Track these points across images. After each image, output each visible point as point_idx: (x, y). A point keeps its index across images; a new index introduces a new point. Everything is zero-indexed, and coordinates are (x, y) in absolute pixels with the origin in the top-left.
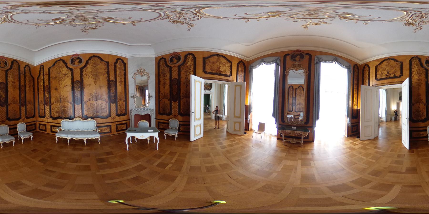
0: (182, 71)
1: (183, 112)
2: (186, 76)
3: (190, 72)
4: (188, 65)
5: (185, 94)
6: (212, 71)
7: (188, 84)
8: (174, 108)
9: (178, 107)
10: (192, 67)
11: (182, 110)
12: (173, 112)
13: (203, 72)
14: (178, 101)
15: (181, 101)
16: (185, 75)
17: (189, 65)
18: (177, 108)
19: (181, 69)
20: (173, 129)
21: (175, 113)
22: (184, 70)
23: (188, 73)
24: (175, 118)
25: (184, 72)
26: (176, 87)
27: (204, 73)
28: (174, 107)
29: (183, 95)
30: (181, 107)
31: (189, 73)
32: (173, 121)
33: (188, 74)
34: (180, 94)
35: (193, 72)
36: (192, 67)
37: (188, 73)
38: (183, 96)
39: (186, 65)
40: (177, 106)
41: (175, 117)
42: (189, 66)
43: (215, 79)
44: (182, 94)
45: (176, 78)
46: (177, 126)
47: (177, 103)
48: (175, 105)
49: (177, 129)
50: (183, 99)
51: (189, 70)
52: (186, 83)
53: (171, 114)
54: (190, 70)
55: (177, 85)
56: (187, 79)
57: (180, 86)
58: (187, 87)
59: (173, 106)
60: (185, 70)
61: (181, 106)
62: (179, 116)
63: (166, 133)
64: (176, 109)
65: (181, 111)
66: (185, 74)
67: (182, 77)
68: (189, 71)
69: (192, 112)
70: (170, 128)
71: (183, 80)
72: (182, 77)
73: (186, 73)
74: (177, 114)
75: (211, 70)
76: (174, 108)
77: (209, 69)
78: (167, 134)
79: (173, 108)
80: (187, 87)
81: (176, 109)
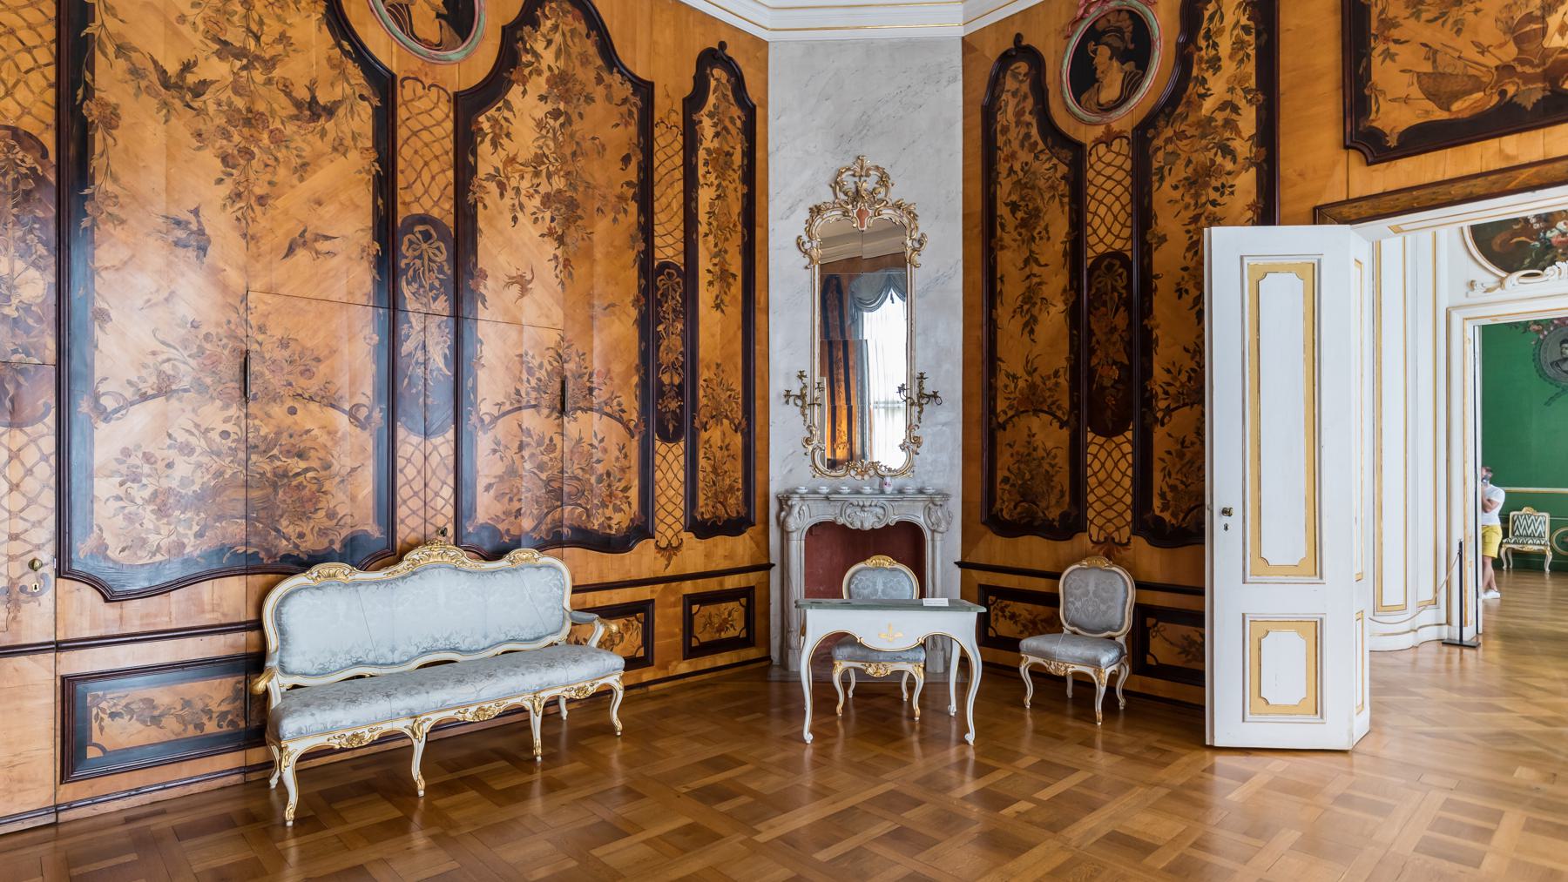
0: (1162, 179)
1: (1174, 515)
4: (1208, 105)
5: (1184, 377)
6: (1444, 102)
8: (1100, 484)
9: (1130, 472)
10: (1240, 124)
11: (1163, 495)
12: (1091, 514)
13: (1346, 147)
14: (1129, 434)
15: (1159, 433)
17: (1224, 106)
18: (1127, 482)
19: (1155, 165)
20: (1088, 631)
21: (1109, 521)
22: (1180, 172)
23: (1214, 195)
24: (1109, 556)
25: (1175, 188)
26: (1121, 320)
27: (1354, 156)
28: (1102, 475)
29: (1169, 384)
30: (1157, 477)
31: (1220, 190)
32: (1092, 579)
33: (1214, 203)
34: (1147, 373)
35: (1253, 170)
36: (1248, 121)
37: (1214, 195)
38: (1172, 390)
39: (1191, 119)
40: (1123, 465)
41: (1111, 550)
42: (1220, 117)
43: (1479, 186)
44: (1167, 378)
45: (1118, 245)
46: (1119, 615)
47: (1127, 448)
48: (1109, 464)
49: (1121, 640)
50: (1169, 411)
51: (1219, 159)
53: (1083, 529)
54: (1229, 166)
55: (1122, 309)
57: (1147, 311)
59: (1096, 465)
60: (1189, 162)
61: (1157, 466)
62: (1140, 543)
63: (1032, 659)
64: (1119, 492)
65: (1157, 503)
66: (1187, 207)
67: (1163, 239)
68: (1220, 171)
70: (1067, 628)
71: (1166, 259)
72: (1163, 239)
73: (1197, 196)
74: (1126, 531)
75: (1431, 96)
76: (1100, 484)
77: (1415, 92)
78: (1040, 661)
79: (1092, 481)
81: (1119, 492)
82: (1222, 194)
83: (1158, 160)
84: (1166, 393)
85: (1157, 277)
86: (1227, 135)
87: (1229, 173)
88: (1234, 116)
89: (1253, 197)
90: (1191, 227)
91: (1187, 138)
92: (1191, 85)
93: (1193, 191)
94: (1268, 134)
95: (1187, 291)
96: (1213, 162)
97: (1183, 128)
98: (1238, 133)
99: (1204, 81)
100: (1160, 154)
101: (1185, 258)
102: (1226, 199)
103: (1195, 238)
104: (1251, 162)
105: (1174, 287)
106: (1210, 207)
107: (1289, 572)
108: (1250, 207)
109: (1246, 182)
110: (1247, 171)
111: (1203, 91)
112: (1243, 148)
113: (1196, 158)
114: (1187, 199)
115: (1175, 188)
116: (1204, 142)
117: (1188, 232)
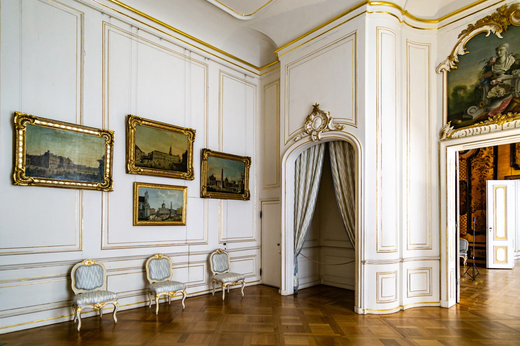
0: (474, 168)
2: (481, 176)
3: (487, 170)
4: (483, 156)
5: (478, 205)
7: (483, 189)
9: (466, 222)
10: (490, 160)
14: (466, 215)
15: (473, 215)
16: (479, 175)
17: (487, 156)
18: (466, 224)
19: (472, 165)
22: (477, 167)
23: (485, 172)
25: (476, 170)
29: (475, 206)
31: (486, 171)
33: (485, 174)
34: (471, 204)
35: (493, 169)
36: (492, 160)
37: (485, 172)
38: (475, 207)
39: (480, 158)
42: (486, 158)
44: (474, 204)
45: (464, 179)
46: (465, 249)
47: (466, 217)
50: (475, 211)
51: (486, 166)
52: (481, 188)
54: (488, 167)
56: (482, 182)
57: (471, 192)
58: (482, 194)
60: (479, 166)
62: (469, 235)
66: (479, 174)
67: (474, 179)
68: (486, 168)
69: (489, 227)
72: (474, 179)
74: (466, 233)
80: (482, 194)
82: (486, 172)
83: (473, 165)
84: (474, 207)
85: (472, 186)
86: (488, 162)
87: (488, 169)
88: (489, 158)
89: (493, 173)
90: (480, 177)
91: (479, 161)
92: (480, 152)
93: (480, 171)
94: (496, 162)
95: (479, 189)
96: (485, 166)
97: (478, 159)
98: (490, 162)
99: (483, 152)
100: (473, 164)
101: (478, 183)
102: (487, 173)
103: (481, 179)
104: (492, 167)
105: (476, 188)
106: (484, 174)
107: (501, 239)
108: (492, 175)
109: (491, 171)
110: (492, 168)
111: (482, 153)
112: (491, 164)
113: (481, 165)
114: (479, 172)
115: (476, 170)
116: (483, 162)
117: (479, 178)
